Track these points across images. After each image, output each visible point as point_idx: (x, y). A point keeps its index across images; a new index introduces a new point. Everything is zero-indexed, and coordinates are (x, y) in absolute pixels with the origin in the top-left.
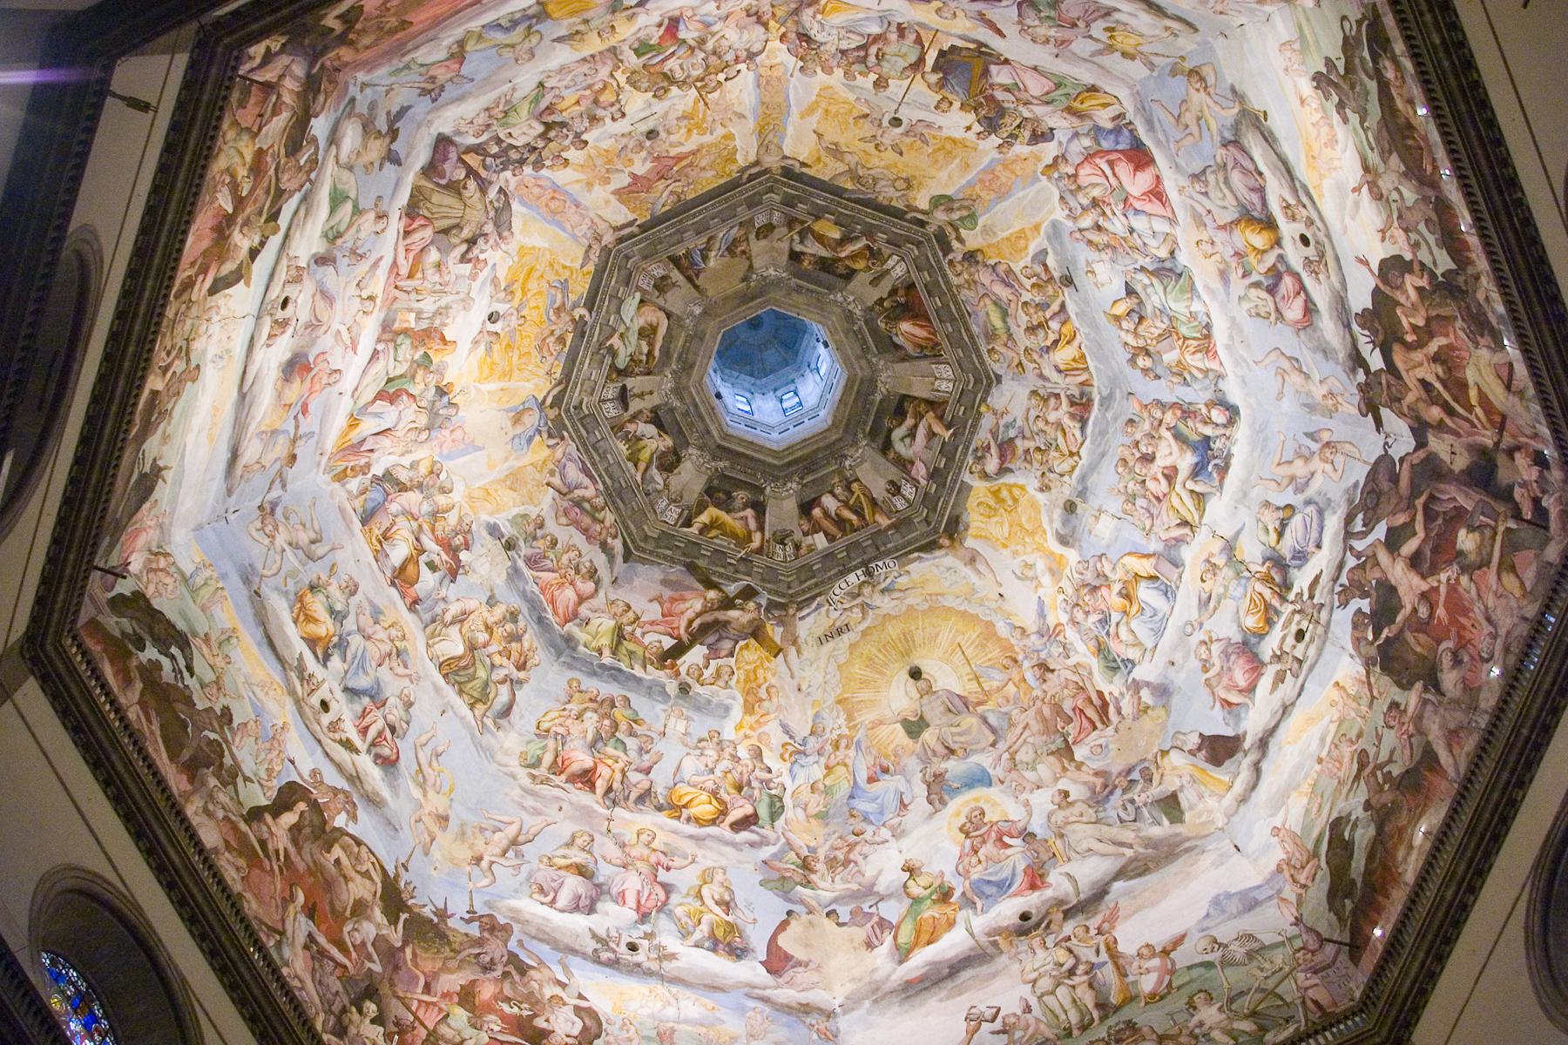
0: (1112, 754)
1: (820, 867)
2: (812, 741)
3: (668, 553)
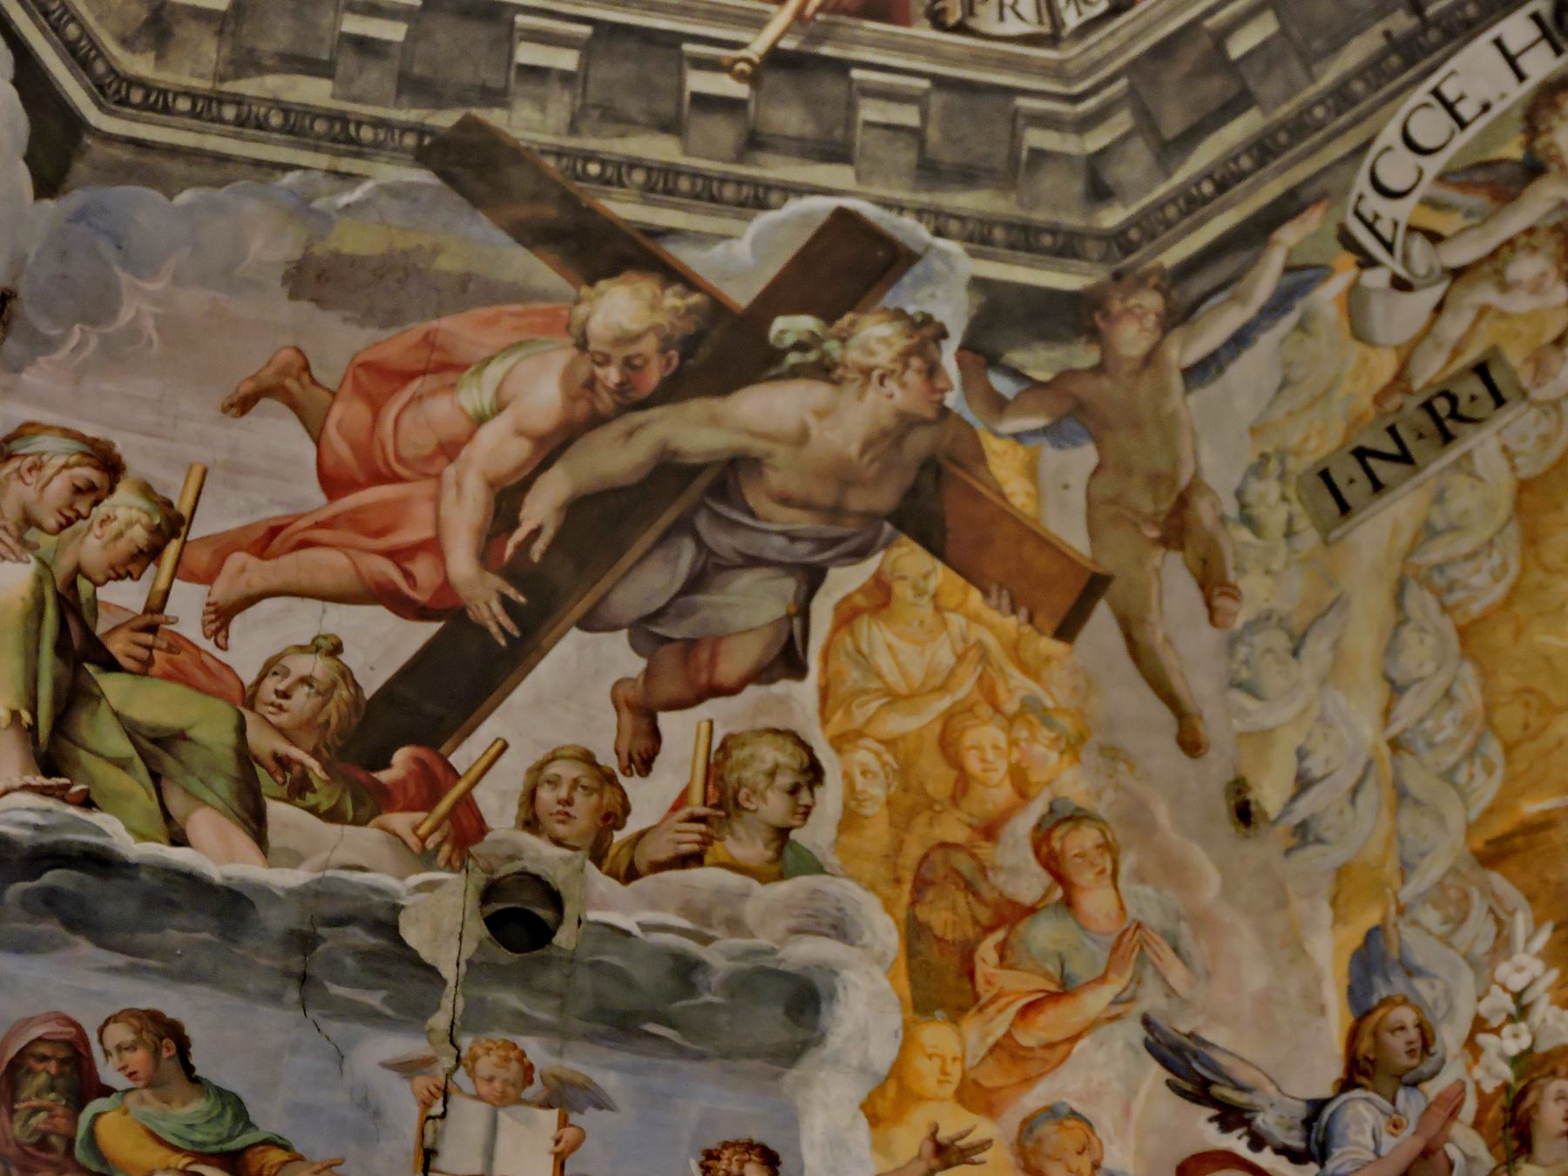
3: (313, 91)
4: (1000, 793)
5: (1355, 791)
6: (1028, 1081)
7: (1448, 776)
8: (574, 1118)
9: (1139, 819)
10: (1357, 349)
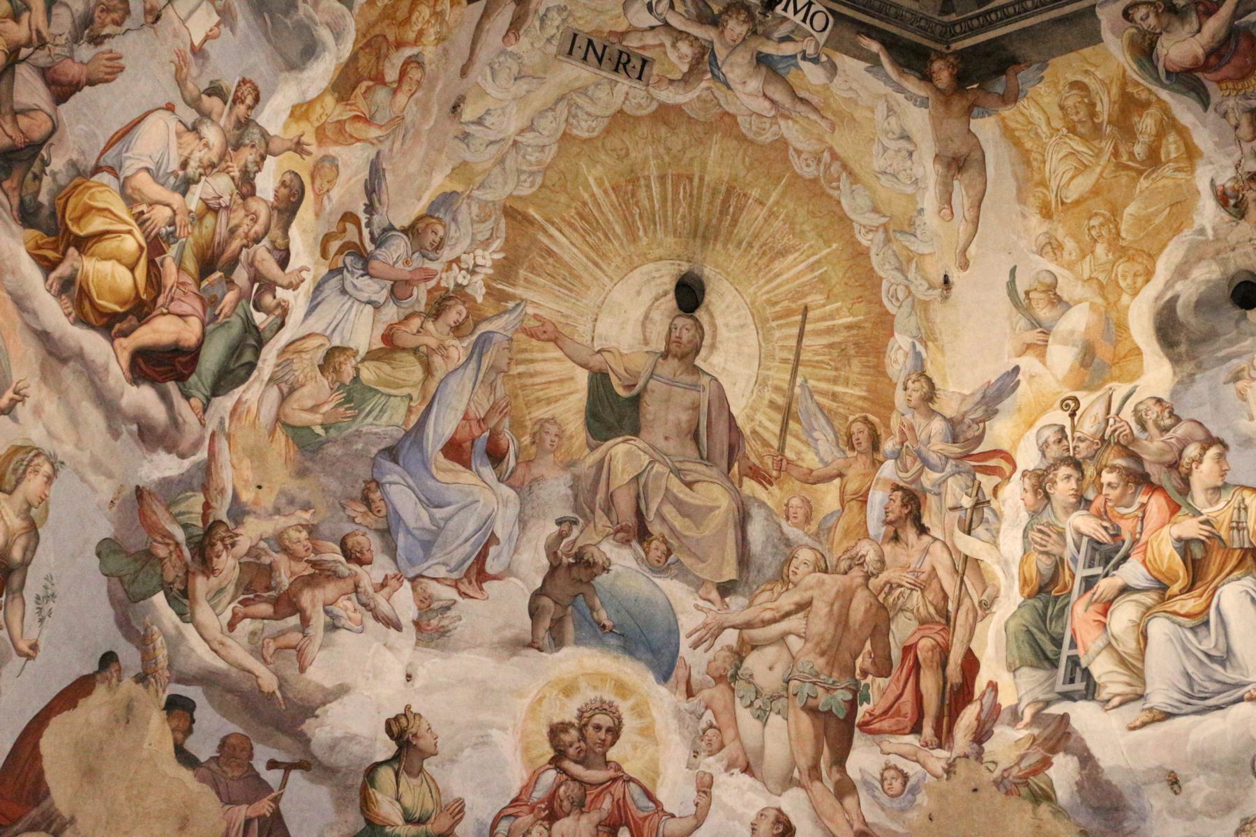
0: (913, 815)
1: (227, 564)
2: (399, 247)
4: (412, 36)
5: (492, 143)
6: (336, 143)
7: (520, 172)
8: (222, 26)
9: (433, 81)
10: (620, 10)
